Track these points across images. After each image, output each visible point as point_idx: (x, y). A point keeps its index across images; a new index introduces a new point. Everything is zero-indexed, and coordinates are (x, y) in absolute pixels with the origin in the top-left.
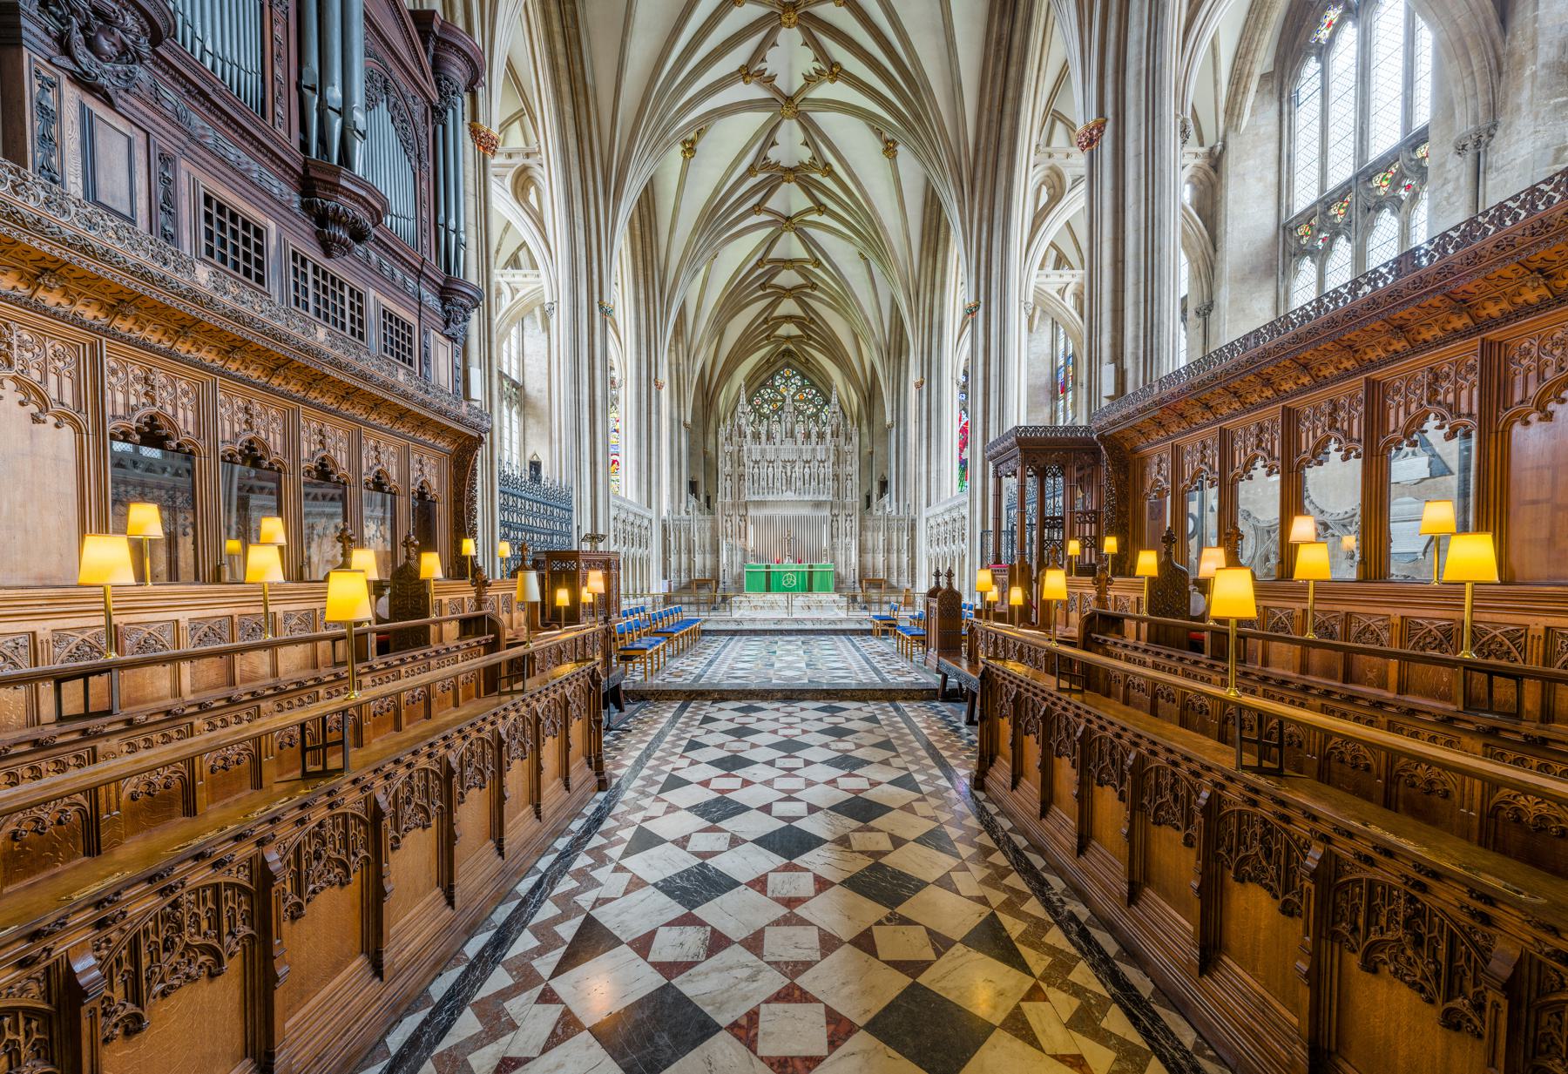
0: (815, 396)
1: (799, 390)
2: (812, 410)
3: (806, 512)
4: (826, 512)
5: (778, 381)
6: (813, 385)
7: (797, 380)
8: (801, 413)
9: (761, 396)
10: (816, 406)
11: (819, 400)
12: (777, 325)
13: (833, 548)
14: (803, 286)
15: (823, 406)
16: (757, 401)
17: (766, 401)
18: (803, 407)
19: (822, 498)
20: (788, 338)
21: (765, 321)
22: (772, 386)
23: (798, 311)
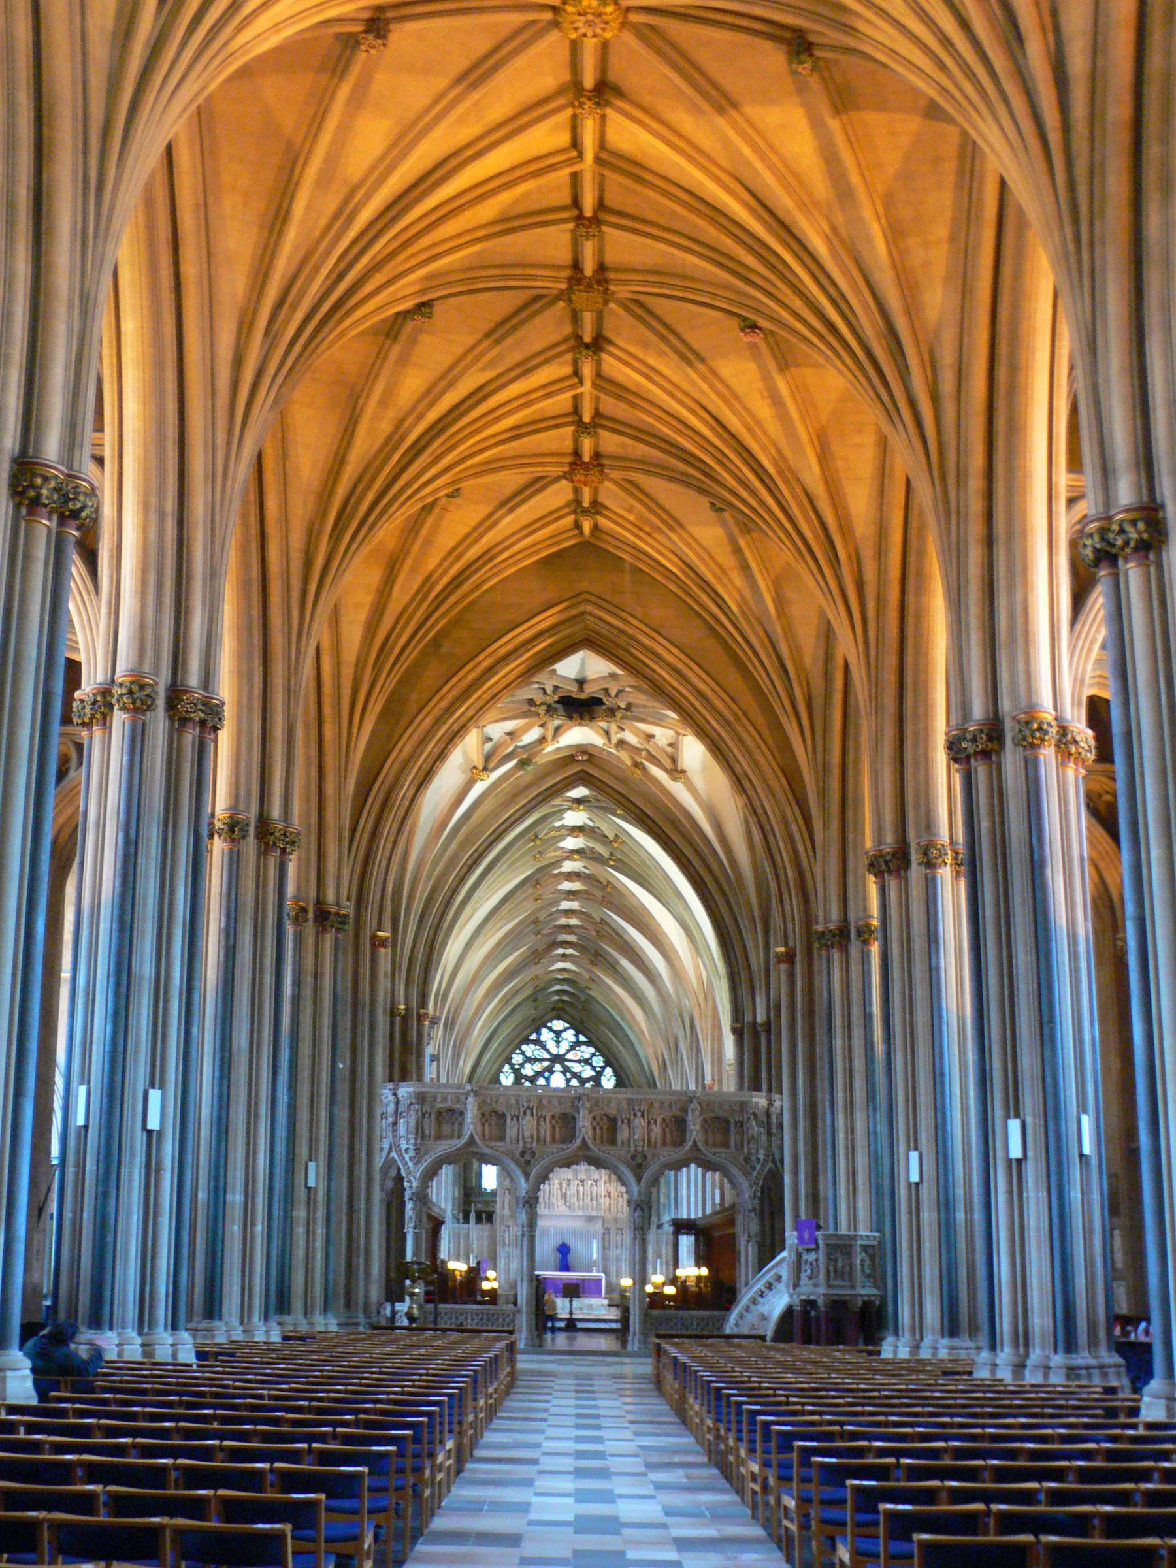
0: (593, 1055)
1: (574, 1046)
2: (588, 1073)
3: (579, 1224)
4: (599, 1227)
5: (546, 1035)
7: (570, 1035)
9: (523, 1053)
11: (598, 1061)
13: (605, 1259)
15: (603, 1068)
16: (517, 1059)
17: (529, 1060)
18: (576, 1068)
19: (594, 1213)
22: (538, 1042)
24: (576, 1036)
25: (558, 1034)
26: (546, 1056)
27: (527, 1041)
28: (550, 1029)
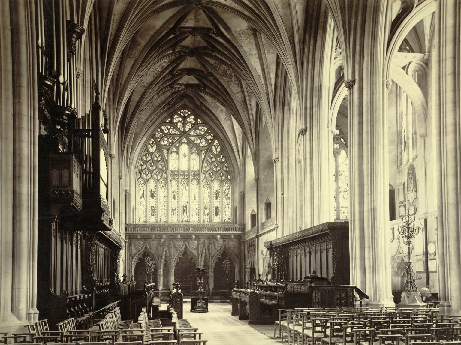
0: (206, 132)
1: (194, 126)
2: (204, 144)
5: (177, 119)
6: (204, 123)
7: (191, 119)
8: (197, 145)
9: (162, 131)
10: (207, 141)
12: (180, 76)
14: (205, 47)
15: (213, 141)
20: (188, 86)
21: (171, 73)
23: (199, 67)
24: (196, 119)
25: (184, 118)
26: (177, 133)
27: (164, 123)
28: (180, 116)
